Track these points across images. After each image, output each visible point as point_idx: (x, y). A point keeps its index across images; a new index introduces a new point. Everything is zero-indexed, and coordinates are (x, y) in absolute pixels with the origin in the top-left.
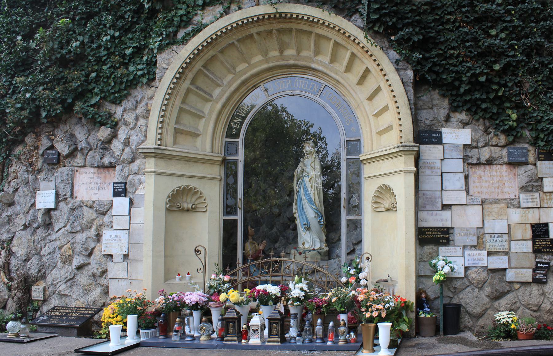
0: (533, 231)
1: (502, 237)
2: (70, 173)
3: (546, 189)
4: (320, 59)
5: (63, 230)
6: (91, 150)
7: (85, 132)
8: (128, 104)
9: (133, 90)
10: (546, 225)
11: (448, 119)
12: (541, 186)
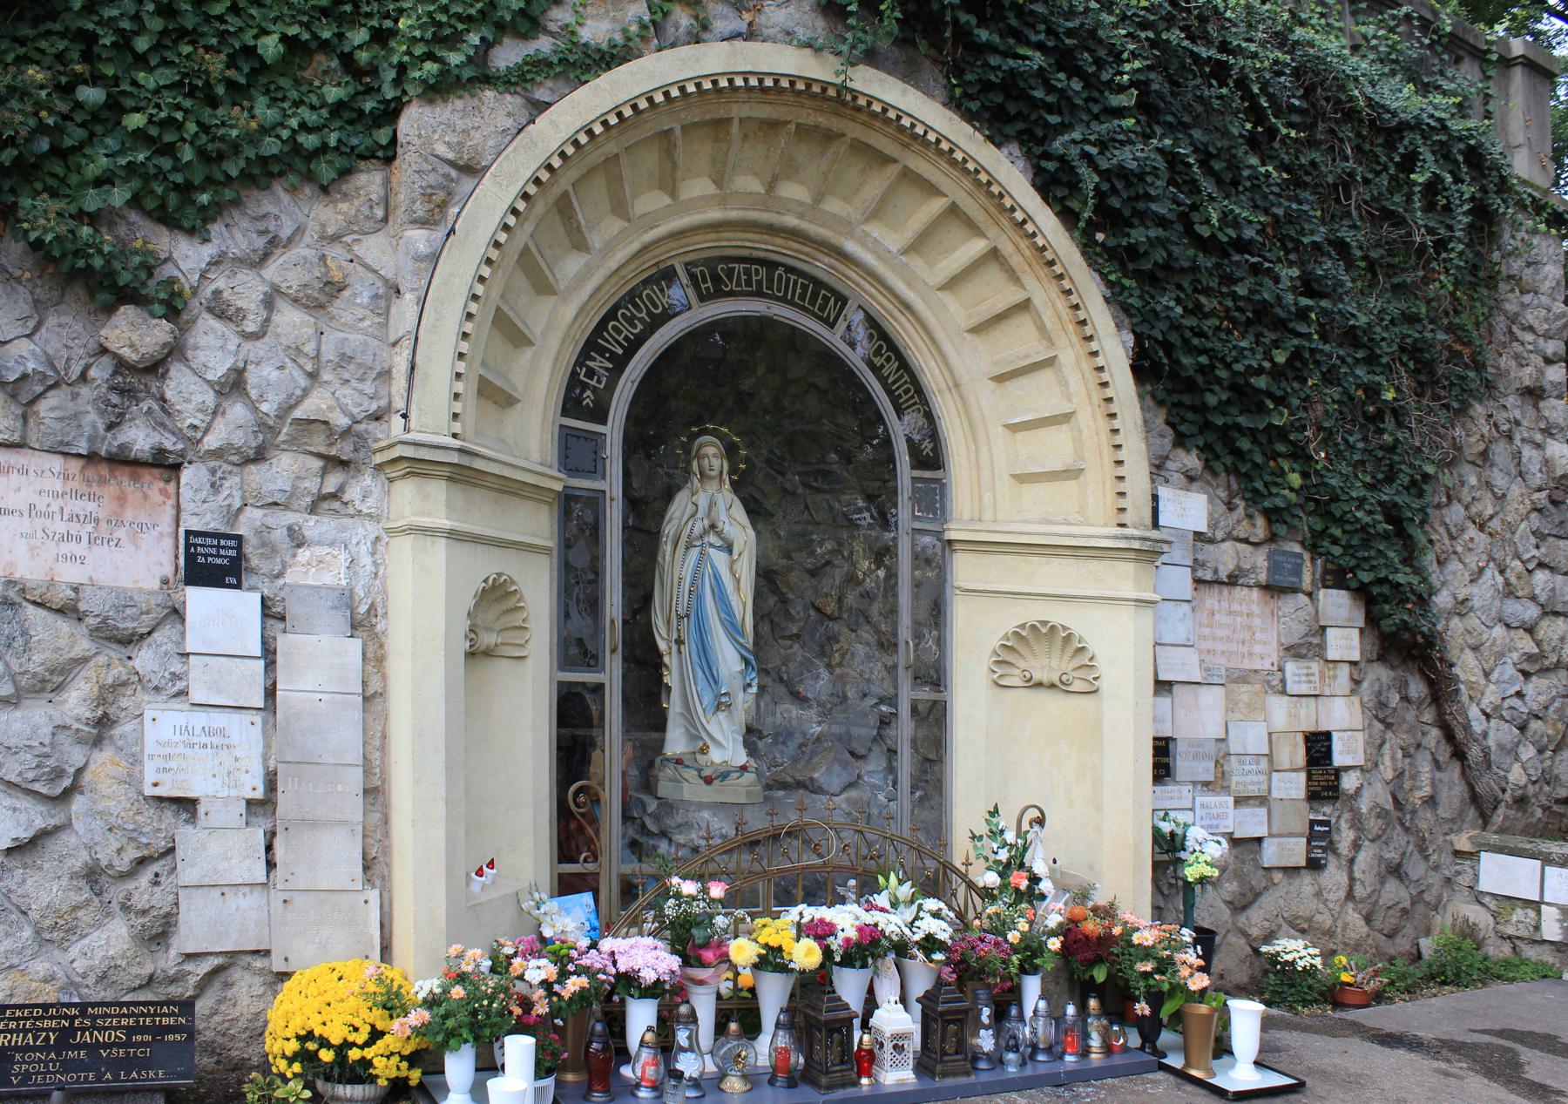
0: (1308, 750)
1: (1258, 763)
4: (875, 234)
6: (56, 386)
7: (25, 308)
8: (232, 236)
9: (255, 192)
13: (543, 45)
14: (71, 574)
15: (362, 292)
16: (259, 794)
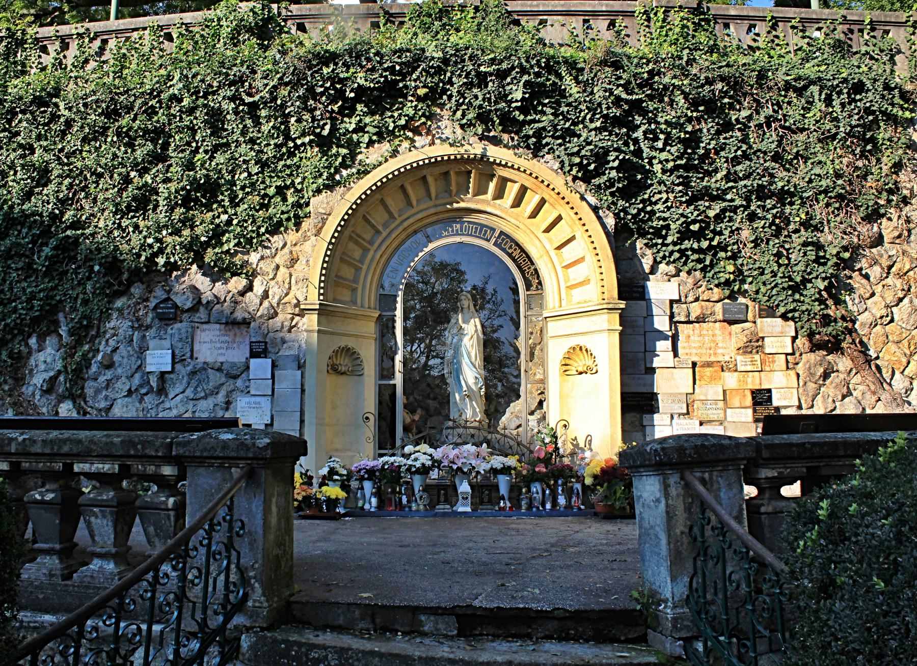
0: (753, 398)
1: (716, 404)
2: (190, 330)
3: (767, 351)
5: (181, 396)
10: (769, 391)
12: (762, 347)
14: (221, 359)
15: (303, 260)
16: (269, 422)
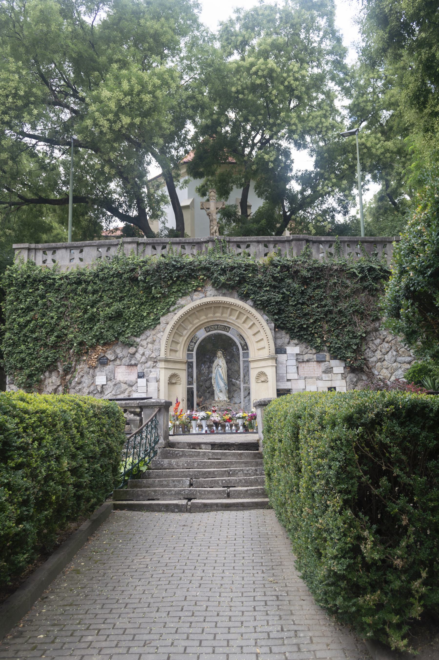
8: (143, 337)
11: (289, 343)
13: (176, 306)
14: (126, 379)
15: (158, 341)
